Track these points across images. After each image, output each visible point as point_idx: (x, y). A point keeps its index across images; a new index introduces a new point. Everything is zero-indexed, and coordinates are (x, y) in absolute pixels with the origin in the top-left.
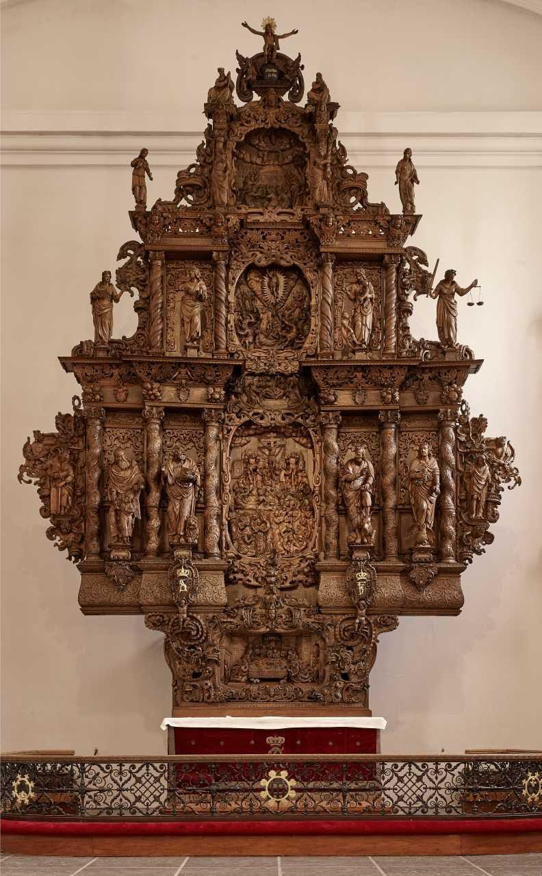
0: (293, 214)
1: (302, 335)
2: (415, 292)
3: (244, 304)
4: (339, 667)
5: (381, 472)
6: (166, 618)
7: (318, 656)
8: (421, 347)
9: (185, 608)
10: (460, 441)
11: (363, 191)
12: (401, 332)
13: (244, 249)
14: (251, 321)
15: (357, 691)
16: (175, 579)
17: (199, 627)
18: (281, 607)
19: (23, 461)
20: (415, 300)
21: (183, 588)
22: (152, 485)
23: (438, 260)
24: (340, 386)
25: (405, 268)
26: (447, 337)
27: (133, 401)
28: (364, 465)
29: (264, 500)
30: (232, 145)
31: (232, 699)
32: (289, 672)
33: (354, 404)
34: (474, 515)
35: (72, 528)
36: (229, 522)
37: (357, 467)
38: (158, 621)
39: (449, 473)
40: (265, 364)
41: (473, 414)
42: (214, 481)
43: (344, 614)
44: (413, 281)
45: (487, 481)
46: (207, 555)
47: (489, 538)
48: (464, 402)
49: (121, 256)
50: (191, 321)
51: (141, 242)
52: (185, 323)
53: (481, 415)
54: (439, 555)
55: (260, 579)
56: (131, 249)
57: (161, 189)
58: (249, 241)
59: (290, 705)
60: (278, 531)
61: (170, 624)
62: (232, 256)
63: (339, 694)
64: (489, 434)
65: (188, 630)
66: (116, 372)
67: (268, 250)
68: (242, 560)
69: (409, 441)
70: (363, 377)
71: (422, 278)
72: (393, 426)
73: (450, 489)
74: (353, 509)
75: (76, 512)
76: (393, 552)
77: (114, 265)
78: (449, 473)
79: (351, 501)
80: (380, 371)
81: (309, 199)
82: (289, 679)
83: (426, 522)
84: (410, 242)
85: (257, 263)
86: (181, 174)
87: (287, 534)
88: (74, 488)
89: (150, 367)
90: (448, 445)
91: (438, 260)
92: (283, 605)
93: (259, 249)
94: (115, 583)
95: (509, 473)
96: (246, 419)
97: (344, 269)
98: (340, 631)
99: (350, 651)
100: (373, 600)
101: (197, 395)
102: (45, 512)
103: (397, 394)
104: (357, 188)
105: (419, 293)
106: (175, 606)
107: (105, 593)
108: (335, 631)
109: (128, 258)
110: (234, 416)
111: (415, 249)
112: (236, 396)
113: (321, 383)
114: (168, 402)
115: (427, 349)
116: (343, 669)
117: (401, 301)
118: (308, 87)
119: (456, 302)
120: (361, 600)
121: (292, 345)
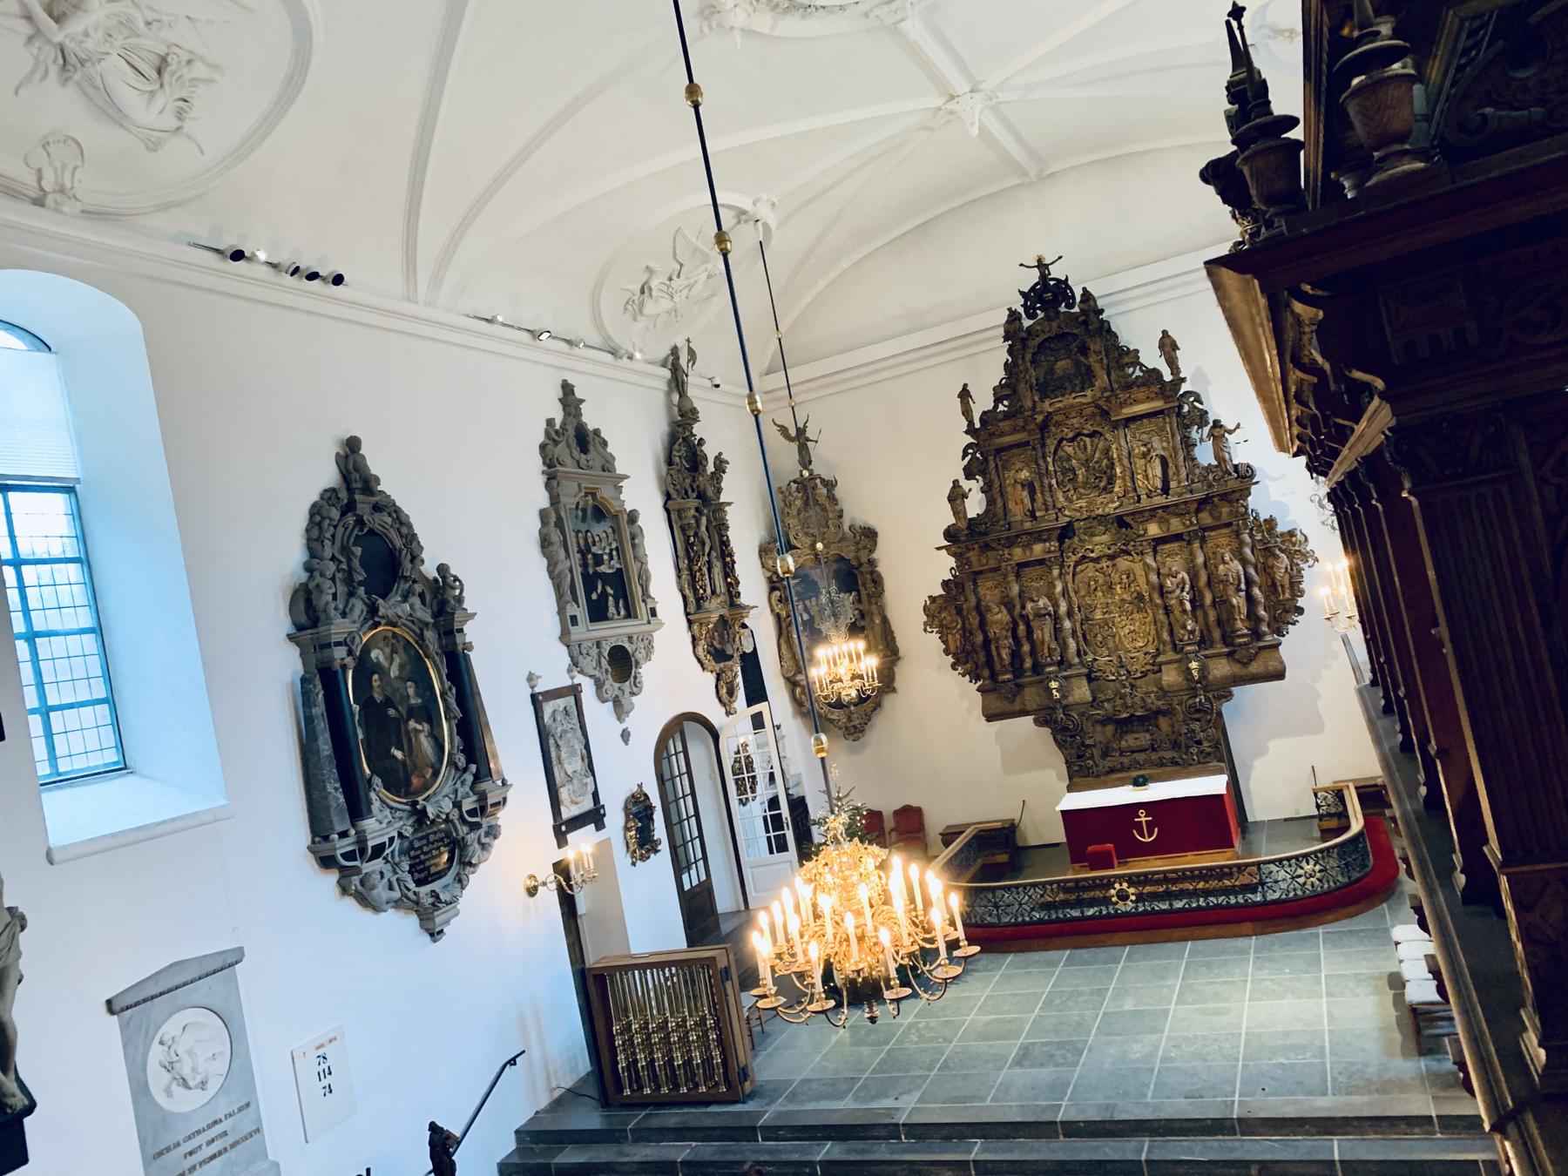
5: (1194, 577)
16: (1049, 690)
19: (925, 618)
27: (993, 564)
30: (1028, 357)
41: (1263, 516)
42: (1063, 608)
46: (1071, 666)
47: (1300, 611)
54: (1256, 635)
57: (983, 402)
59: (1159, 771)
64: (1281, 528)
75: (968, 647)
78: (1252, 571)
82: (1154, 749)
87: (1133, 636)
94: (1007, 698)
95: (1305, 556)
101: (1038, 549)
102: (947, 652)
106: (1054, 709)
107: (999, 705)
118: (1078, 299)
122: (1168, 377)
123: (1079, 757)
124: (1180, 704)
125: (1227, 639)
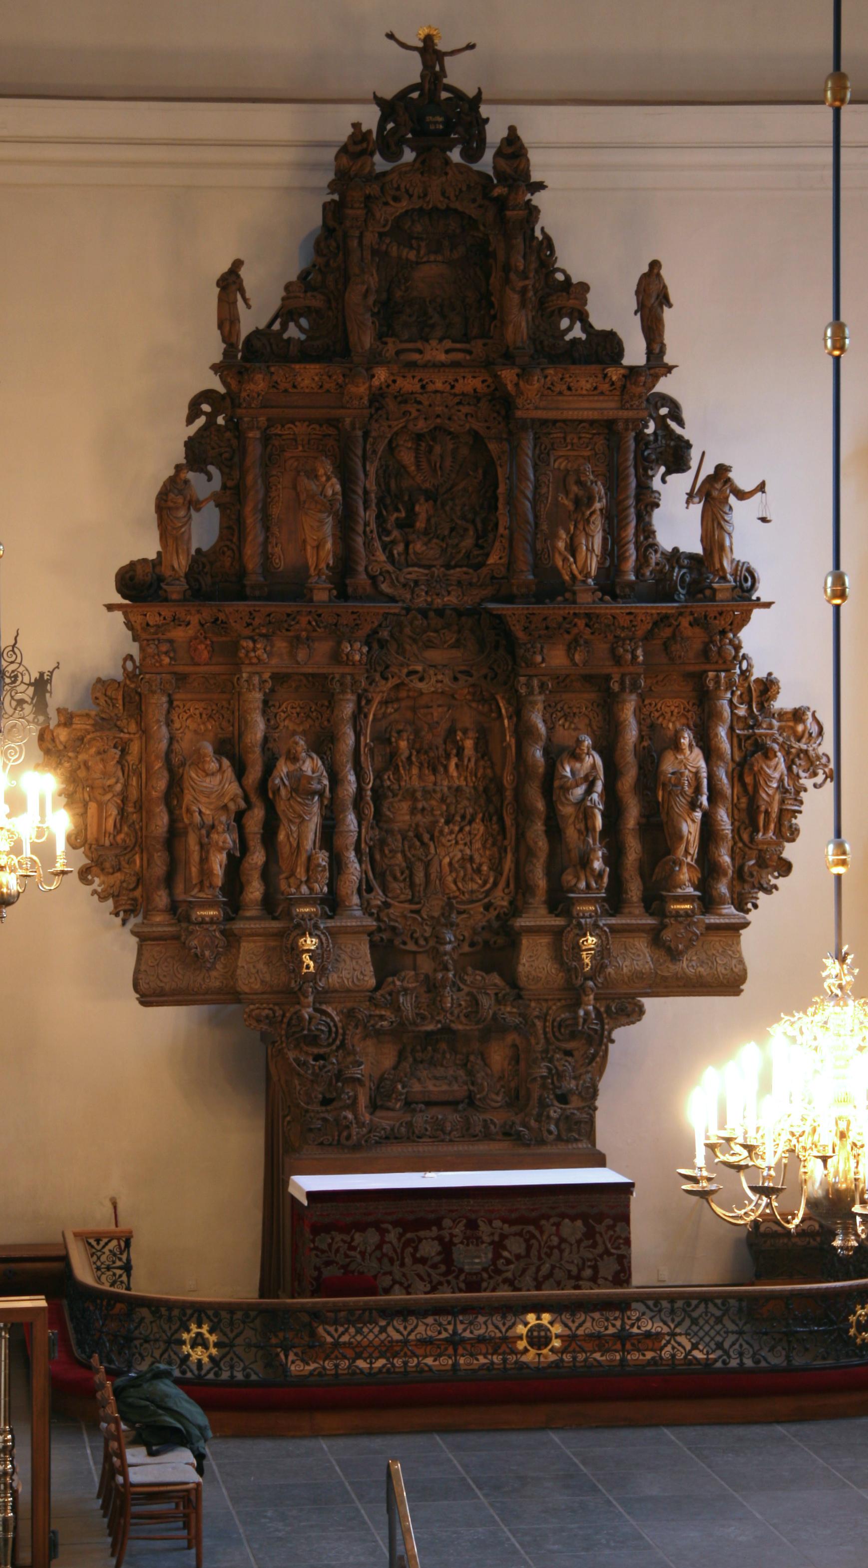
1: (483, 542)
2: (663, 469)
4: (553, 1083)
6: (279, 1013)
7: (518, 1062)
9: (311, 999)
10: (739, 717)
15: (579, 1122)
16: (296, 952)
17: (332, 1024)
18: (459, 990)
20: (664, 481)
21: (308, 967)
22: (254, 798)
28: (588, 761)
29: (423, 809)
31: (387, 1138)
32: (470, 1091)
34: (761, 834)
35: (120, 864)
36: (370, 848)
37: (578, 765)
38: (267, 1017)
39: (722, 774)
40: (427, 593)
41: (758, 673)
43: (559, 1000)
44: (661, 453)
45: (781, 780)
48: (744, 657)
49: (194, 412)
53: (770, 674)
55: (422, 942)
60: (447, 860)
61: (286, 1020)
63: (552, 1127)
65: (318, 1033)
68: (391, 910)
69: (657, 714)
72: (634, 697)
73: (724, 797)
74: (571, 833)
76: (635, 899)
78: (722, 774)
79: (571, 820)
83: (687, 852)
88: (122, 801)
90: (721, 729)
92: (462, 986)
96: (396, 681)
98: (553, 1027)
99: (570, 1059)
100: (605, 978)
105: (669, 472)
108: (545, 1027)
110: (378, 677)
116: (560, 1088)
120: (587, 979)
122: (635, 353)
123: (326, 1102)
124: (544, 1018)
125: (655, 899)
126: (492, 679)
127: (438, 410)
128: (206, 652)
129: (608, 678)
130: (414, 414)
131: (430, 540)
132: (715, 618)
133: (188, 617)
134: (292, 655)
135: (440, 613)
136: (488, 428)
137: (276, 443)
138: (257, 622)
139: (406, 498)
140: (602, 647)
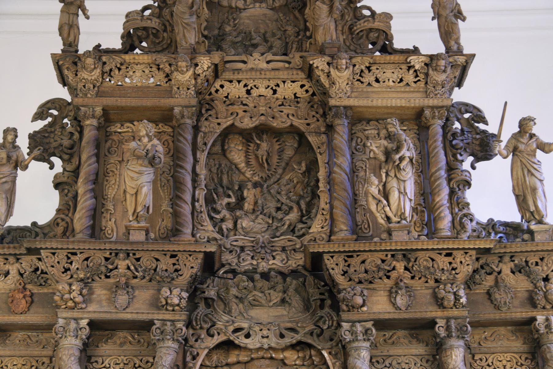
0: (289, 63)
1: (306, 216)
3: (221, 180)
8: (491, 231)
11: (387, 34)
12: (457, 210)
13: (220, 107)
14: (230, 200)
20: (473, 168)
23: (506, 103)
24: (371, 282)
25: (454, 127)
26: (532, 208)
33: (393, 310)
40: (252, 258)
44: (468, 144)
49: (40, 115)
50: (136, 194)
51: (69, 99)
52: (128, 196)
56: (55, 109)
58: (227, 97)
62: (203, 115)
66: (13, 269)
67: (255, 107)
70: (406, 269)
71: (482, 140)
77: (27, 127)
80: (433, 260)
81: (311, 44)
84: (458, 96)
85: (238, 124)
86: (130, 15)
89: (69, 258)
91: (506, 103)
93: (241, 106)
96: (222, 338)
97: (365, 130)
103: (462, 293)
104: (378, 30)
105: (478, 159)
109: (50, 119)
111: (467, 105)
112: (208, 306)
113: (340, 280)
114: (95, 312)
115: (500, 233)
117: (451, 169)
119: (539, 161)
121: (293, 231)
126: (318, 336)
127: (262, 109)
128: (23, 301)
129: (431, 324)
130: (241, 114)
131: (257, 217)
132: (537, 264)
133: (7, 267)
134: (112, 301)
135: (265, 276)
136: (308, 124)
137: (115, 138)
138: (74, 267)
139: (236, 188)
140: (422, 289)
